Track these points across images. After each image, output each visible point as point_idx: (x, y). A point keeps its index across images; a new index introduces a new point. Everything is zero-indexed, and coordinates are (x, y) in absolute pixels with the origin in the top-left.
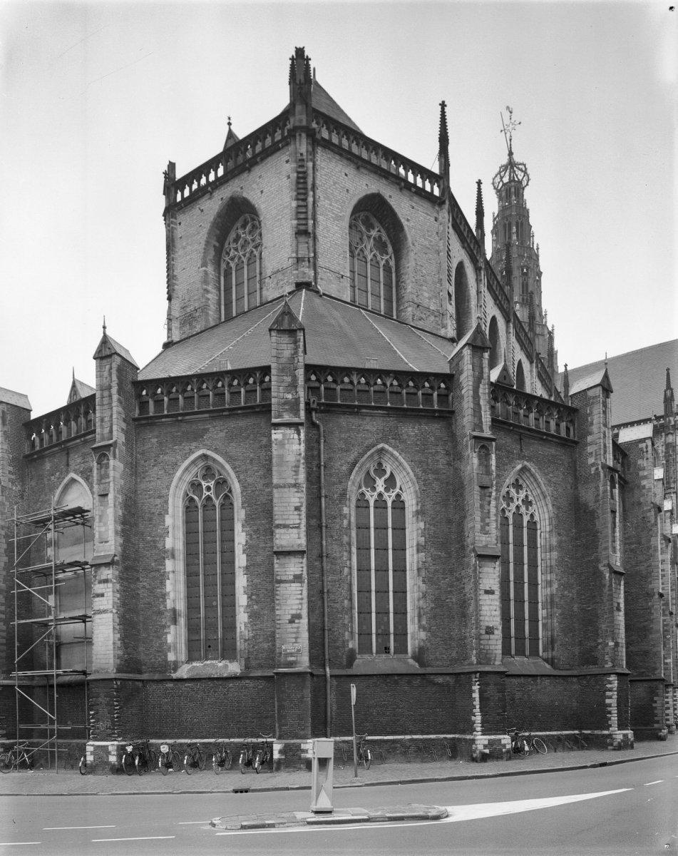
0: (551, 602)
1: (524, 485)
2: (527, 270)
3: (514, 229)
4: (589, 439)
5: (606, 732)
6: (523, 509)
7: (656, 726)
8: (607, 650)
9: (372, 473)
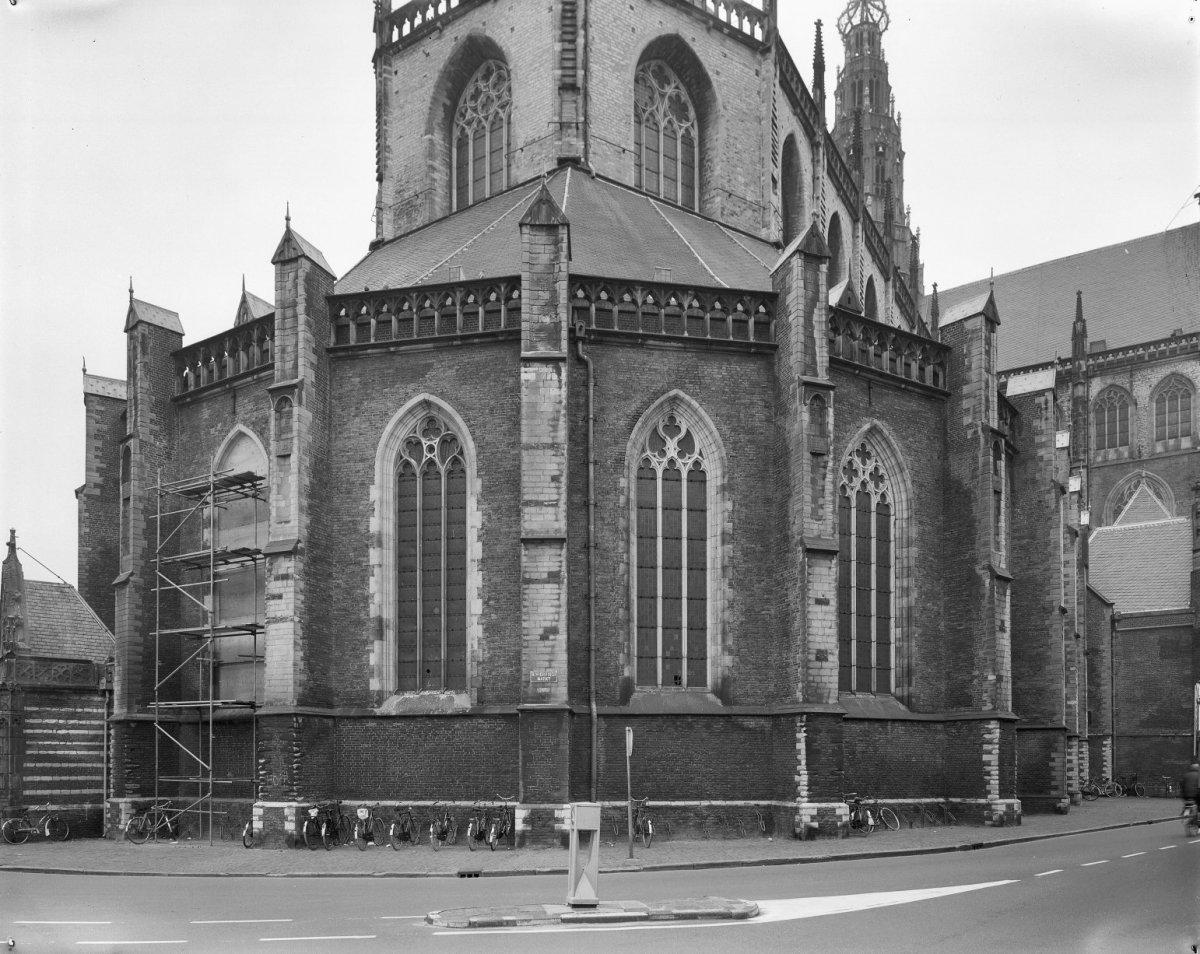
0: (908, 617)
1: (873, 453)
2: (884, 149)
3: (867, 91)
4: (966, 389)
5: (982, 801)
6: (871, 486)
7: (1054, 793)
8: (986, 685)
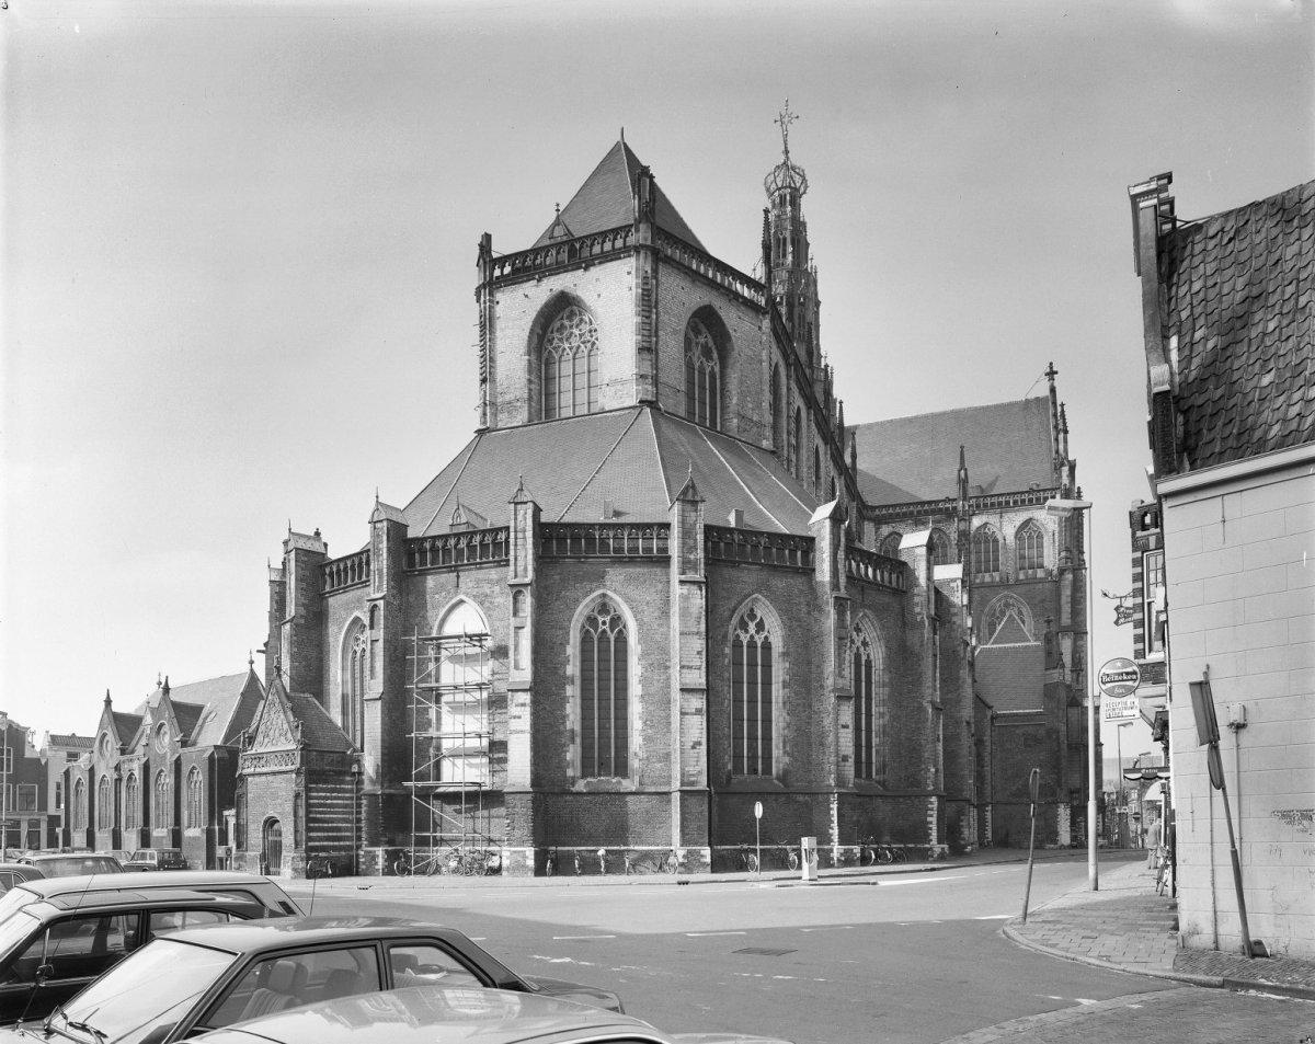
0: (884, 732)
5: (927, 846)
8: (930, 775)
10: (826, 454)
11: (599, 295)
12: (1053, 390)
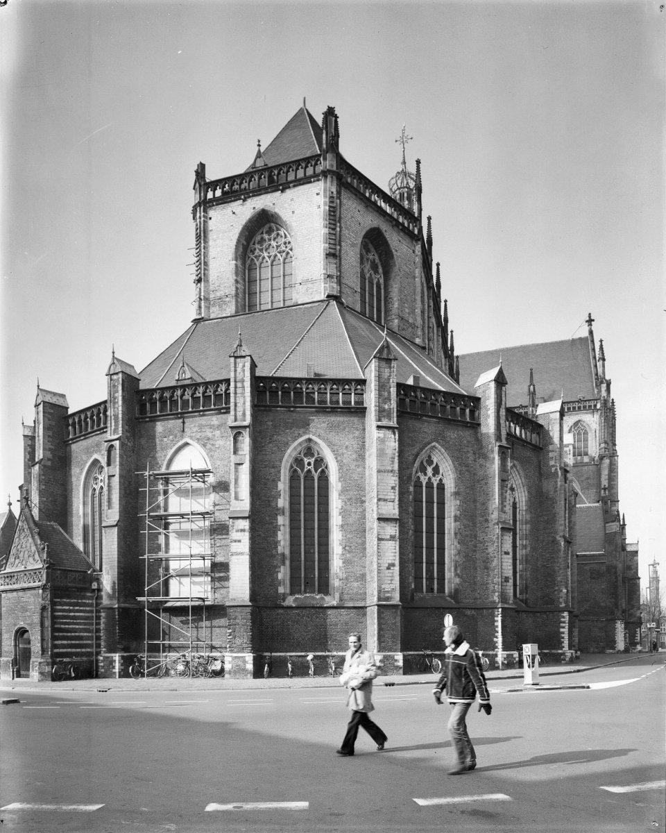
4: (551, 447)
5: (560, 651)
8: (562, 594)
9: (425, 463)
10: (445, 365)
11: (293, 212)
12: (591, 332)
